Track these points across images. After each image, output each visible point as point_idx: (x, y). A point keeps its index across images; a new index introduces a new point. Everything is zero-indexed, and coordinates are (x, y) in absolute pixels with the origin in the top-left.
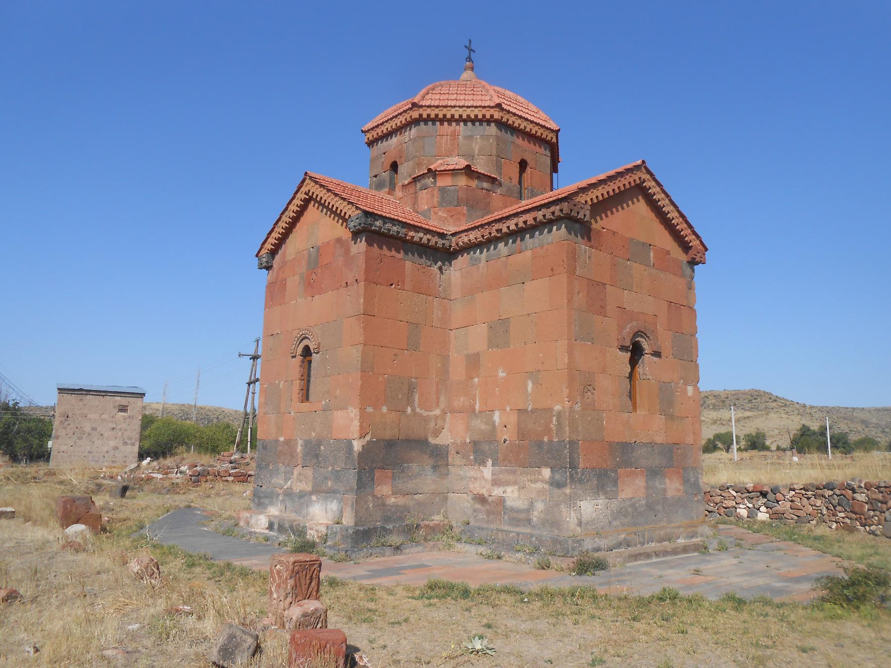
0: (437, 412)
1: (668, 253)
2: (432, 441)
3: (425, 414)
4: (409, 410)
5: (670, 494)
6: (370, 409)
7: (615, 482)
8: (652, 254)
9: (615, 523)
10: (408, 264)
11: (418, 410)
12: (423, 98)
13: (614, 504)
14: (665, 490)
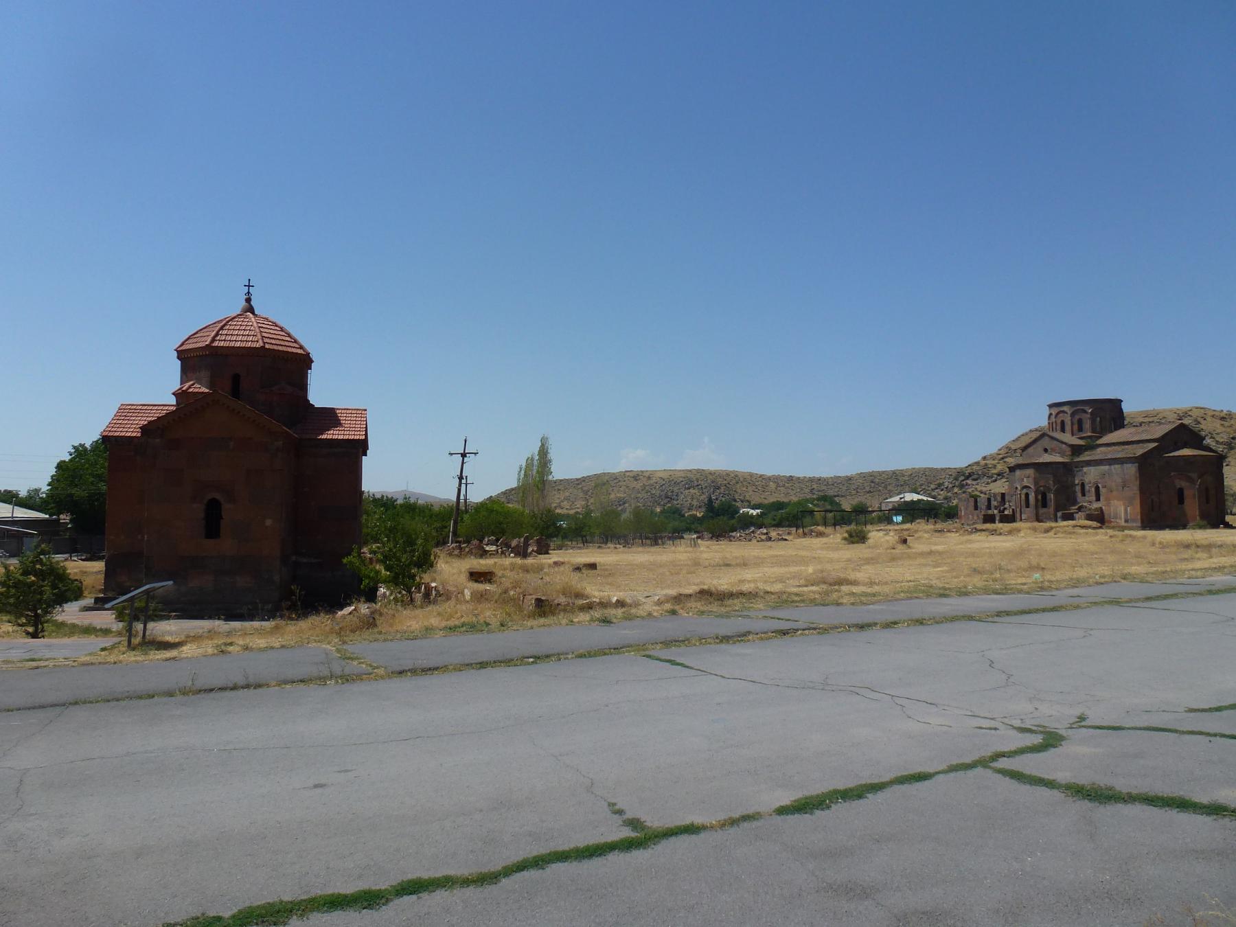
12: (182, 344)
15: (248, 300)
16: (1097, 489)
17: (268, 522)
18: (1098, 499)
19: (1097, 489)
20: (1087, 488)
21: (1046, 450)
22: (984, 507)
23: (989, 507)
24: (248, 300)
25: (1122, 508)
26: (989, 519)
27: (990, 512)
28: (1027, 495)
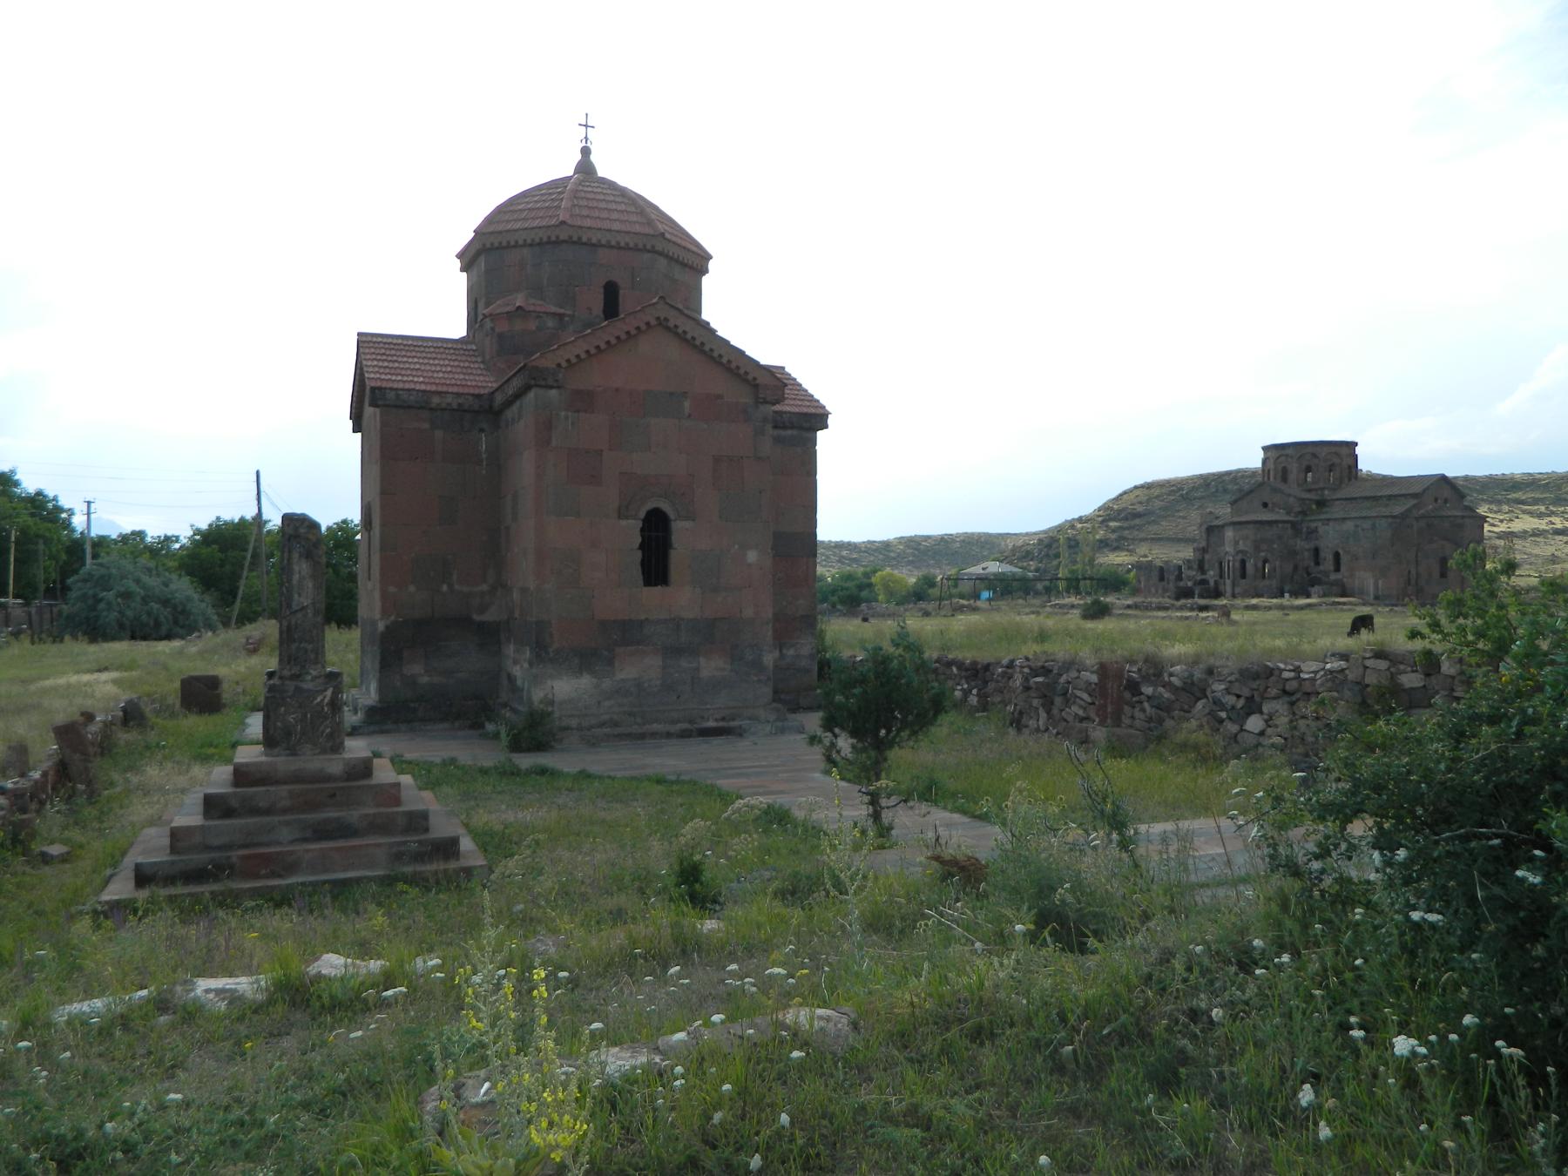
0: (485, 587)
1: (720, 397)
2: (477, 618)
3: (465, 589)
4: (445, 588)
5: (705, 674)
6: (392, 589)
7: (610, 662)
8: (687, 404)
9: (607, 703)
10: (439, 434)
11: (457, 587)
13: (607, 684)
14: (697, 669)
15: (586, 152)
16: (1337, 556)
17: (752, 556)
18: (1337, 569)
19: (1337, 556)
20: (1322, 555)
21: (1265, 505)
22: (1172, 578)
23: (1179, 578)
24: (586, 152)
25: (1371, 581)
26: (1186, 593)
27: (1181, 584)
28: (1243, 562)
